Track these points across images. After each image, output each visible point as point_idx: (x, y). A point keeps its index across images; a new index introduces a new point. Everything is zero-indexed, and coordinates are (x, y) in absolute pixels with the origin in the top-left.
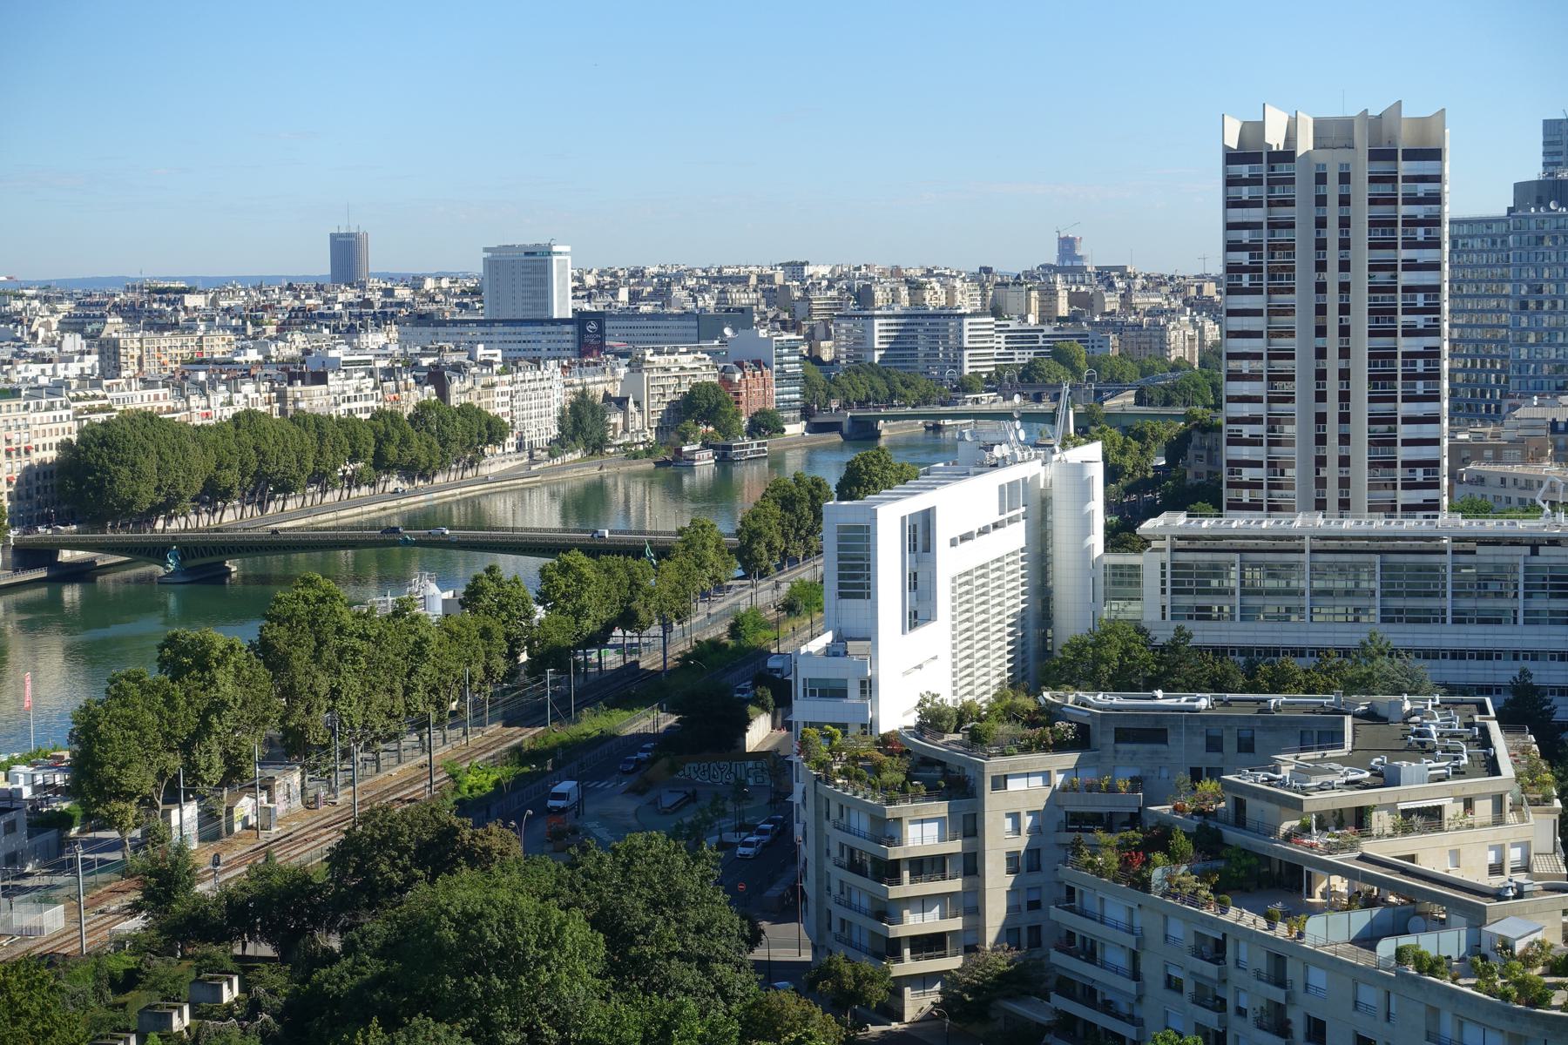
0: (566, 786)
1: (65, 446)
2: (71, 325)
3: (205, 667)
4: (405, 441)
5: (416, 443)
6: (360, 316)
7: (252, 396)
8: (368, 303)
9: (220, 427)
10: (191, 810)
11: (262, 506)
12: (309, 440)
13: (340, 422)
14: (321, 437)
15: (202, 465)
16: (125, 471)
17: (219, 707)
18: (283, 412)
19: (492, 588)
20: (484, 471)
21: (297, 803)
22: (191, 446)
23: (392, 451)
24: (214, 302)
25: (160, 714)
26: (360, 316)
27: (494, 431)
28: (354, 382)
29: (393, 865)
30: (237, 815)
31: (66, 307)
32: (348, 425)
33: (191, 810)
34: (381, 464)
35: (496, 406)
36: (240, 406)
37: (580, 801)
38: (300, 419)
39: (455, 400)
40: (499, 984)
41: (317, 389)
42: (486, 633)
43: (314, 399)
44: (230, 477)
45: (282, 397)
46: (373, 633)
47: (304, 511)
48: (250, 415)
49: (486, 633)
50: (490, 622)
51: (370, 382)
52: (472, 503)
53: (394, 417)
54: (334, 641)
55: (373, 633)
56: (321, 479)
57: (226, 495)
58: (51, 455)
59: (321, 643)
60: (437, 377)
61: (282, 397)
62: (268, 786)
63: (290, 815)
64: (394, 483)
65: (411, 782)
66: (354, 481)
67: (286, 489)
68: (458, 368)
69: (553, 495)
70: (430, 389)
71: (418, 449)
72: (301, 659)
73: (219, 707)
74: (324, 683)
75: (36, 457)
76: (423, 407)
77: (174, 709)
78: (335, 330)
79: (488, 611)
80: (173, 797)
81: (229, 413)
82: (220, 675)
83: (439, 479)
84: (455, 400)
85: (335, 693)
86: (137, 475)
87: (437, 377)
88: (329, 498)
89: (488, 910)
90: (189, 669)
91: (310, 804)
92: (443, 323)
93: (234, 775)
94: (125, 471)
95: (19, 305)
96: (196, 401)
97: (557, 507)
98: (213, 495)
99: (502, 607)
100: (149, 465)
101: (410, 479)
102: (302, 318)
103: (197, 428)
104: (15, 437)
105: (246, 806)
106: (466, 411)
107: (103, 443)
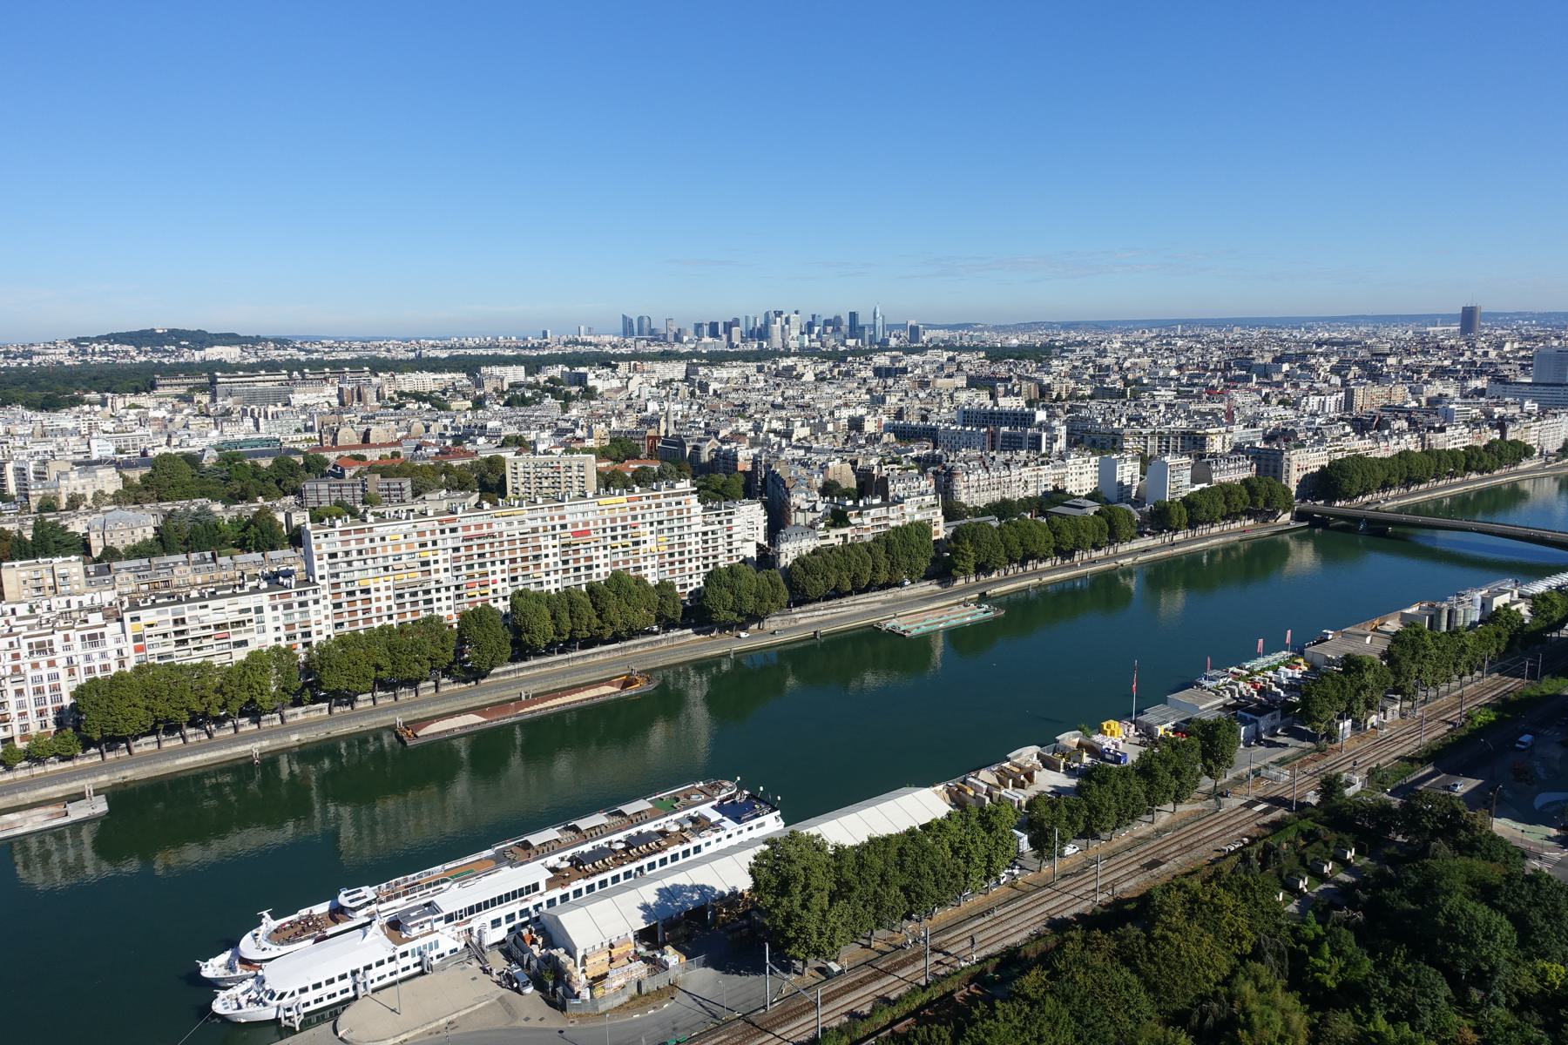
0: (1526, 738)
1: (1323, 467)
2: (1335, 370)
3: (1360, 671)
4: (1481, 459)
5: (1486, 458)
6: (1469, 372)
7: (1410, 443)
8: (1474, 363)
9: (1391, 459)
10: (1348, 723)
11: (1408, 488)
12: (1434, 462)
13: (1450, 452)
14: (1439, 460)
15: (1381, 475)
16: (1347, 481)
17: (1365, 687)
18: (1423, 446)
19: (1504, 613)
20: (1521, 467)
21: (1397, 717)
22: (1377, 469)
23: (1474, 464)
24: (1400, 362)
25: (1338, 691)
26: (1469, 372)
27: (1527, 451)
28: (1459, 431)
29: (1429, 821)
30: (1369, 722)
31: (1334, 360)
32: (1453, 453)
33: (1348, 723)
34: (1468, 468)
35: (1531, 439)
36: (1403, 447)
37: (1533, 745)
38: (1429, 452)
39: (1508, 438)
40: (1462, 950)
41: (1440, 435)
42: (1498, 635)
43: (1441, 441)
44: (1394, 480)
45: (1423, 438)
46: (1441, 646)
47: (1428, 491)
48: (1407, 452)
49: (1498, 635)
50: (1502, 630)
51: (1467, 430)
52: (1514, 484)
53: (1476, 448)
54: (1422, 652)
55: (1441, 646)
56: (1438, 478)
57: (1392, 487)
58: (1316, 470)
59: (1416, 653)
60: (1501, 425)
61: (1423, 438)
62: (1384, 710)
63: (1394, 722)
64: (1474, 476)
65: (1452, 708)
66: (1453, 475)
67: (1420, 482)
68: (1513, 420)
69: (1556, 479)
70: (1497, 431)
71: (1487, 461)
72: (1405, 663)
73: (1365, 687)
74: (1415, 668)
75: (1309, 471)
76: (1492, 442)
77: (1344, 688)
78: (1456, 379)
79: (1501, 624)
80: (1341, 717)
81: (1397, 447)
82: (1367, 675)
83: (1496, 472)
84: (1510, 436)
85: (1420, 671)
86: (1352, 482)
87: (1501, 425)
88: (1440, 483)
89: (1462, 915)
90: (1352, 671)
91: (1402, 715)
92: (1510, 384)
93: (1370, 706)
94: (1347, 481)
95: (1313, 361)
96: (1382, 444)
97: (1556, 485)
98: (1386, 486)
99: (1508, 623)
100: (1358, 478)
101: (1482, 473)
102: (1440, 373)
103: (1381, 459)
104: (1301, 463)
105: (1373, 719)
106: (1514, 443)
107: (1339, 468)
